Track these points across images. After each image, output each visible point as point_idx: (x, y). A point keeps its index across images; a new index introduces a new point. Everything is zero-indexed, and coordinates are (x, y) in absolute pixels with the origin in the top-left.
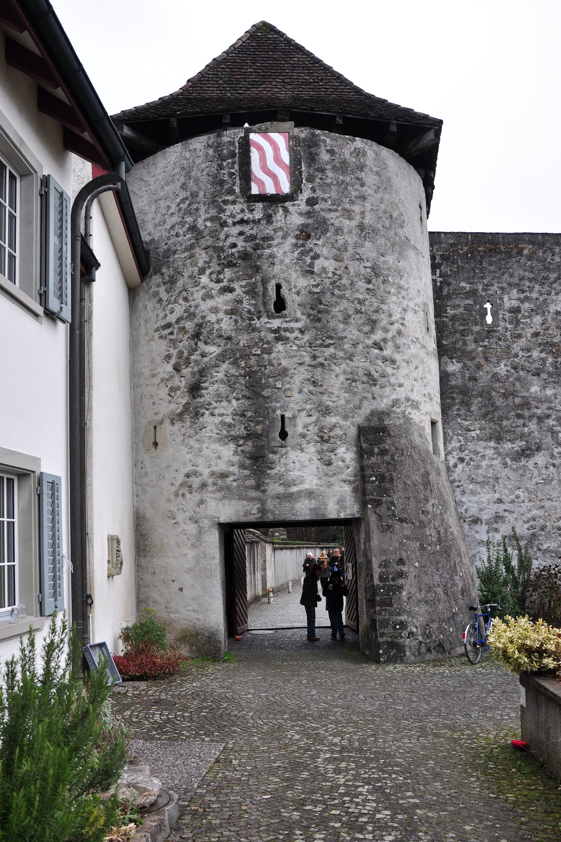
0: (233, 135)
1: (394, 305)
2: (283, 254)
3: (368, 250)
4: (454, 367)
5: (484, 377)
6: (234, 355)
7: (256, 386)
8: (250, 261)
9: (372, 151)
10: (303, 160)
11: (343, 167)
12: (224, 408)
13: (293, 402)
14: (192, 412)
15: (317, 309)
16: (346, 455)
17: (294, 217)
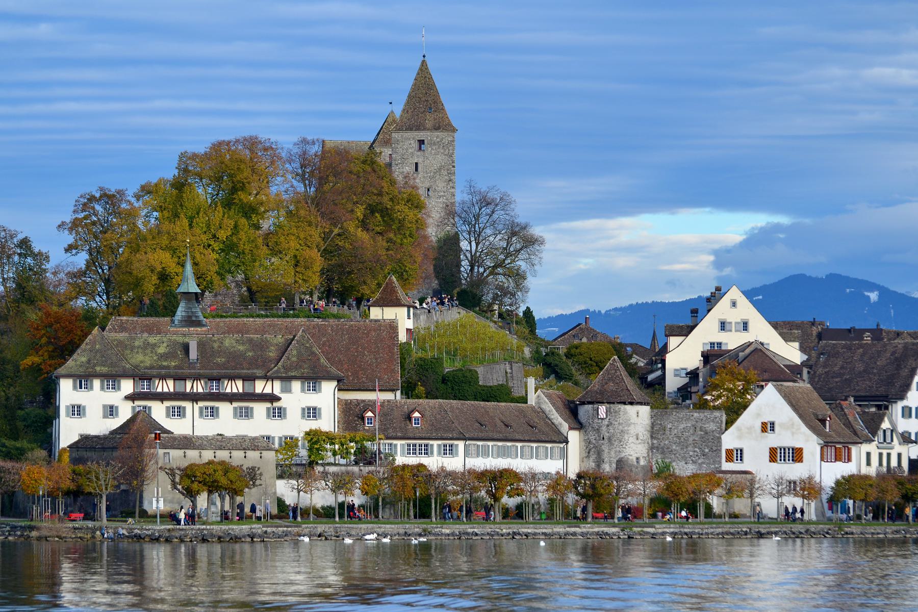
0: (596, 406)
1: (626, 437)
2: (604, 428)
3: (621, 427)
4: (655, 442)
5: (662, 444)
6: (595, 447)
7: (599, 453)
8: (598, 430)
9: (622, 407)
11: (616, 412)
12: (593, 457)
13: (605, 456)
14: (588, 457)
15: (610, 439)
16: (614, 465)
17: (606, 422)
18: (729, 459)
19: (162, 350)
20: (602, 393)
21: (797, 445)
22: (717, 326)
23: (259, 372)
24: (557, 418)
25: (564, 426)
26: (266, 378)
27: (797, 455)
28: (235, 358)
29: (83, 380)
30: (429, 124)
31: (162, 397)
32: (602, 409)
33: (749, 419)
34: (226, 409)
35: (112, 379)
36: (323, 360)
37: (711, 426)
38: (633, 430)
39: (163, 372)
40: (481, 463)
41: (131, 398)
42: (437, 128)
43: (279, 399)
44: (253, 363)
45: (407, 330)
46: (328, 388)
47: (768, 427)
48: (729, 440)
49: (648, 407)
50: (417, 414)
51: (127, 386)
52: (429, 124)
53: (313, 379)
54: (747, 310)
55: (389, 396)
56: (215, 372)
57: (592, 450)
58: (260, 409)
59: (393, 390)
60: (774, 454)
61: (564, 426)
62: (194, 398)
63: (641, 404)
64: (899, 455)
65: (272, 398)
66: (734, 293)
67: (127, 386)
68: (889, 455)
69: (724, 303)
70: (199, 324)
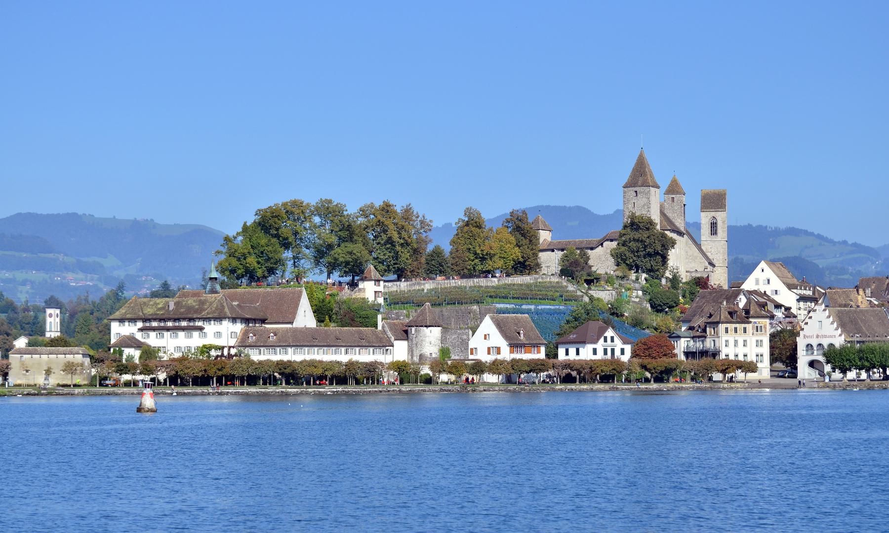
10: (416, 330)
13: (414, 352)
18: (472, 354)
19: (160, 306)
22: (754, 282)
24: (389, 334)
26: (199, 319)
28: (190, 309)
29: (121, 321)
30: (640, 183)
31: (154, 329)
32: (413, 329)
33: (480, 332)
34: (181, 334)
35: (133, 320)
38: (427, 339)
40: (308, 357)
41: (141, 330)
42: (642, 186)
44: (196, 311)
49: (440, 328)
52: (640, 183)
53: (219, 319)
54: (769, 273)
55: (289, 326)
56: (176, 317)
57: (411, 351)
58: (196, 334)
59: (292, 323)
65: (201, 329)
66: (763, 264)
67: (140, 324)
69: (758, 269)
70: (216, 292)
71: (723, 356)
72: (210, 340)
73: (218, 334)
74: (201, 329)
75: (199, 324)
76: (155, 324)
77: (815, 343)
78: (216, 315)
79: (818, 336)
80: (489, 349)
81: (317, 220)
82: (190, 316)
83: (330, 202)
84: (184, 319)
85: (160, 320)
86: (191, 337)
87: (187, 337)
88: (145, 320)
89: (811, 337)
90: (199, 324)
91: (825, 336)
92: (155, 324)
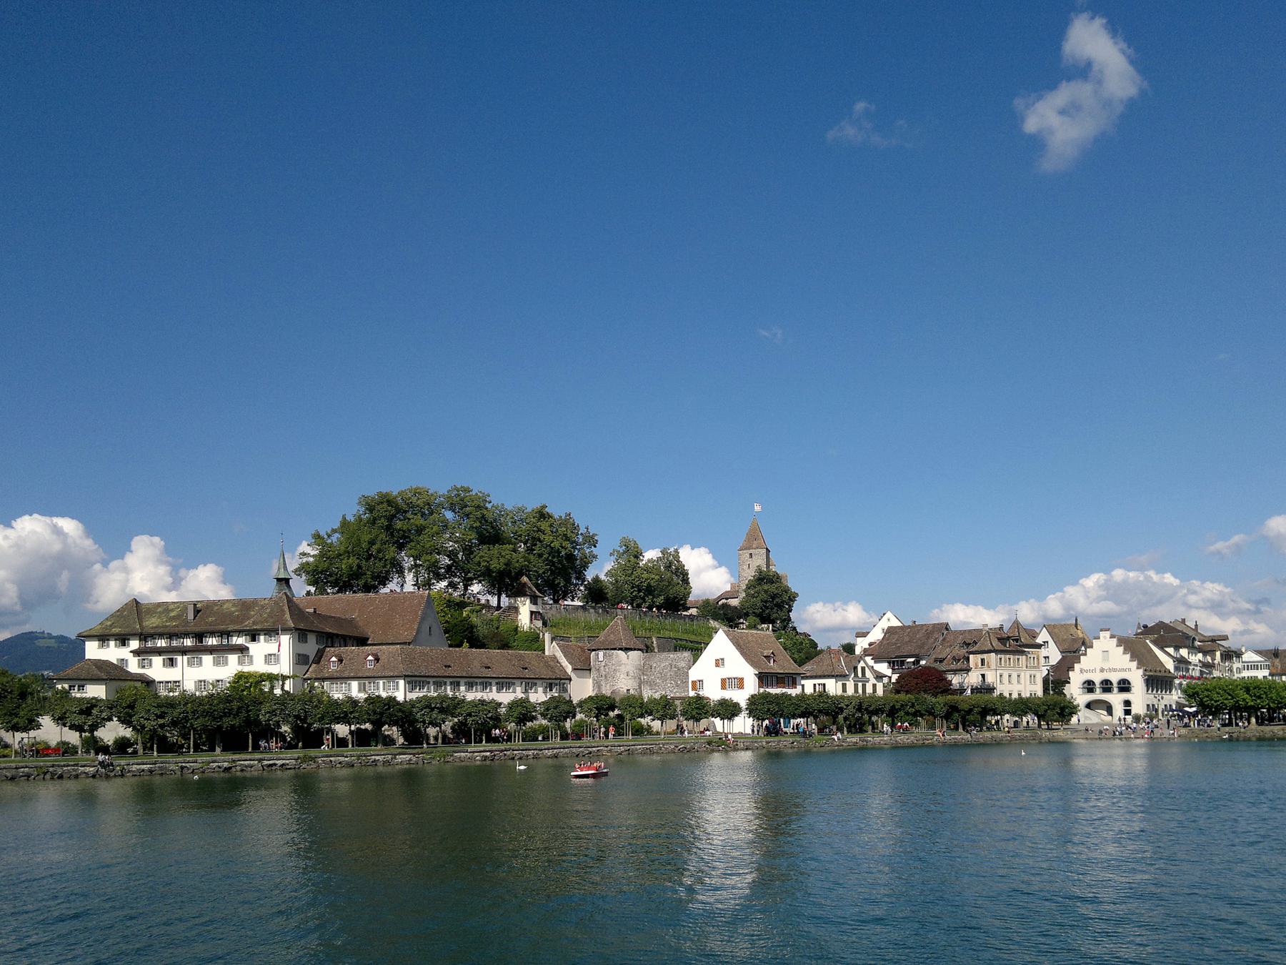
7: (599, 687)
8: (598, 670)
20: (603, 642)
21: (740, 676)
23: (231, 628)
25: (569, 669)
26: (240, 633)
27: (740, 683)
31: (159, 652)
32: (601, 654)
34: (208, 659)
36: (288, 616)
37: (682, 664)
38: (623, 669)
39: (160, 630)
41: (136, 653)
43: (247, 649)
45: (532, 613)
46: (285, 639)
47: (719, 663)
48: (694, 674)
50: (370, 658)
51: (134, 644)
53: (272, 632)
57: (597, 685)
58: (233, 658)
60: (724, 684)
61: (569, 669)
62: (184, 651)
63: (627, 650)
64: (874, 686)
65: (242, 650)
67: (134, 644)
68: (864, 686)
71: (997, 693)
72: (258, 666)
73: (269, 658)
74: (242, 650)
75: (239, 640)
76: (161, 643)
77: (1097, 678)
78: (266, 626)
79: (1102, 670)
80: (723, 681)
81: (449, 515)
82: (222, 627)
83: (467, 490)
84: (212, 634)
85: (171, 636)
86: (226, 663)
87: (216, 663)
88: (143, 637)
89: (1093, 671)
90: (239, 640)
91: (1115, 670)
92: (161, 643)
